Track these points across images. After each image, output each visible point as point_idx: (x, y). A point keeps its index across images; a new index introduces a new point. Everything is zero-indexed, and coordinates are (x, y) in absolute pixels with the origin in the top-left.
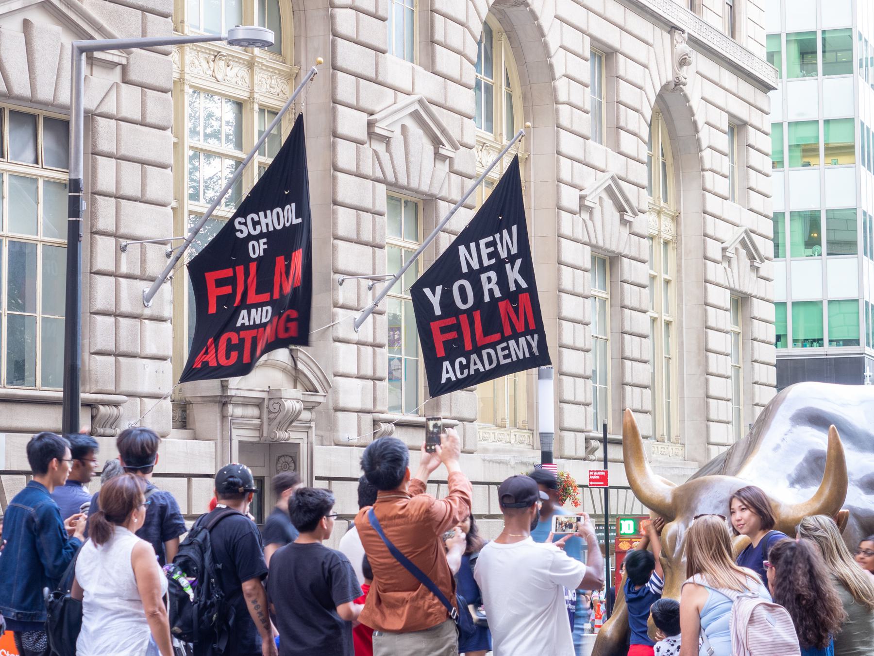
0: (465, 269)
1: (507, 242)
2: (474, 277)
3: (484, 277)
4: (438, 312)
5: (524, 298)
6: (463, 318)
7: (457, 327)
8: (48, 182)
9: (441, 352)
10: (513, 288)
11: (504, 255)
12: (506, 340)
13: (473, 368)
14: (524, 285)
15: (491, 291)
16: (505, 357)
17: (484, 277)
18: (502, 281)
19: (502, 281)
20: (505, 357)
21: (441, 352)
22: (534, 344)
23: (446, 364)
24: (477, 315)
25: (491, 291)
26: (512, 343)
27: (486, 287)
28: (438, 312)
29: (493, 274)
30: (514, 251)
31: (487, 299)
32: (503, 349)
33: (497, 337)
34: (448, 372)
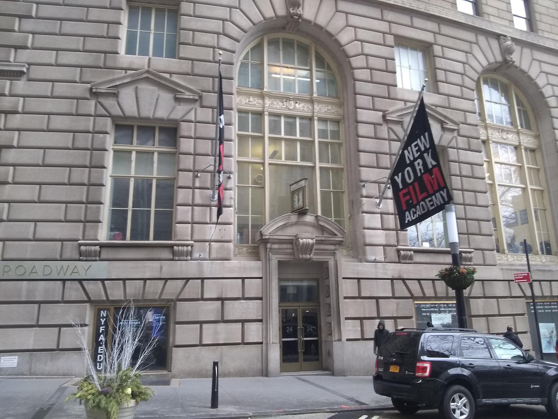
0: (408, 162)
1: (422, 143)
2: (412, 165)
3: (416, 163)
4: (401, 187)
5: (436, 170)
6: (411, 187)
7: (408, 193)
8: (160, 153)
9: (404, 208)
10: (430, 167)
11: (423, 149)
12: (431, 196)
13: (418, 213)
14: (434, 163)
15: (420, 169)
16: (432, 205)
17: (416, 163)
18: (425, 164)
19: (425, 164)
20: (432, 205)
21: (404, 208)
22: (445, 195)
23: (407, 213)
24: (416, 184)
25: (420, 169)
26: (434, 197)
27: (418, 168)
28: (401, 187)
29: (419, 161)
30: (428, 146)
31: (419, 175)
32: (430, 201)
33: (425, 194)
34: (409, 217)
